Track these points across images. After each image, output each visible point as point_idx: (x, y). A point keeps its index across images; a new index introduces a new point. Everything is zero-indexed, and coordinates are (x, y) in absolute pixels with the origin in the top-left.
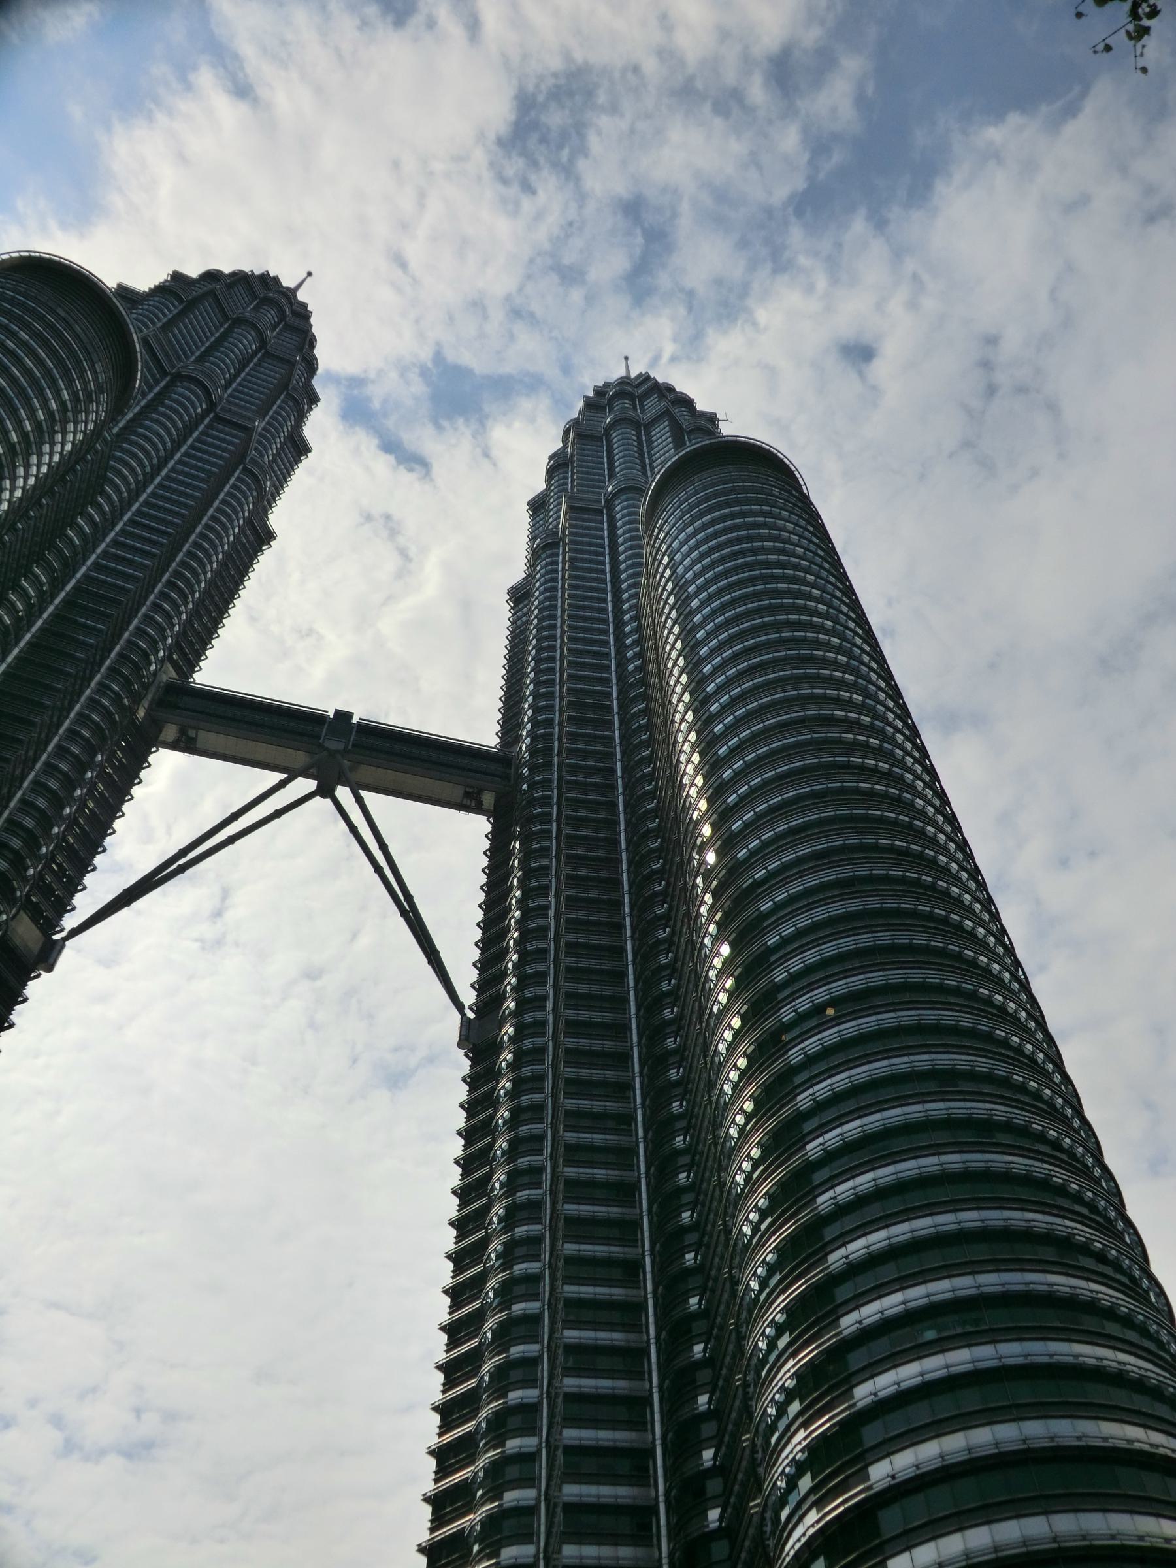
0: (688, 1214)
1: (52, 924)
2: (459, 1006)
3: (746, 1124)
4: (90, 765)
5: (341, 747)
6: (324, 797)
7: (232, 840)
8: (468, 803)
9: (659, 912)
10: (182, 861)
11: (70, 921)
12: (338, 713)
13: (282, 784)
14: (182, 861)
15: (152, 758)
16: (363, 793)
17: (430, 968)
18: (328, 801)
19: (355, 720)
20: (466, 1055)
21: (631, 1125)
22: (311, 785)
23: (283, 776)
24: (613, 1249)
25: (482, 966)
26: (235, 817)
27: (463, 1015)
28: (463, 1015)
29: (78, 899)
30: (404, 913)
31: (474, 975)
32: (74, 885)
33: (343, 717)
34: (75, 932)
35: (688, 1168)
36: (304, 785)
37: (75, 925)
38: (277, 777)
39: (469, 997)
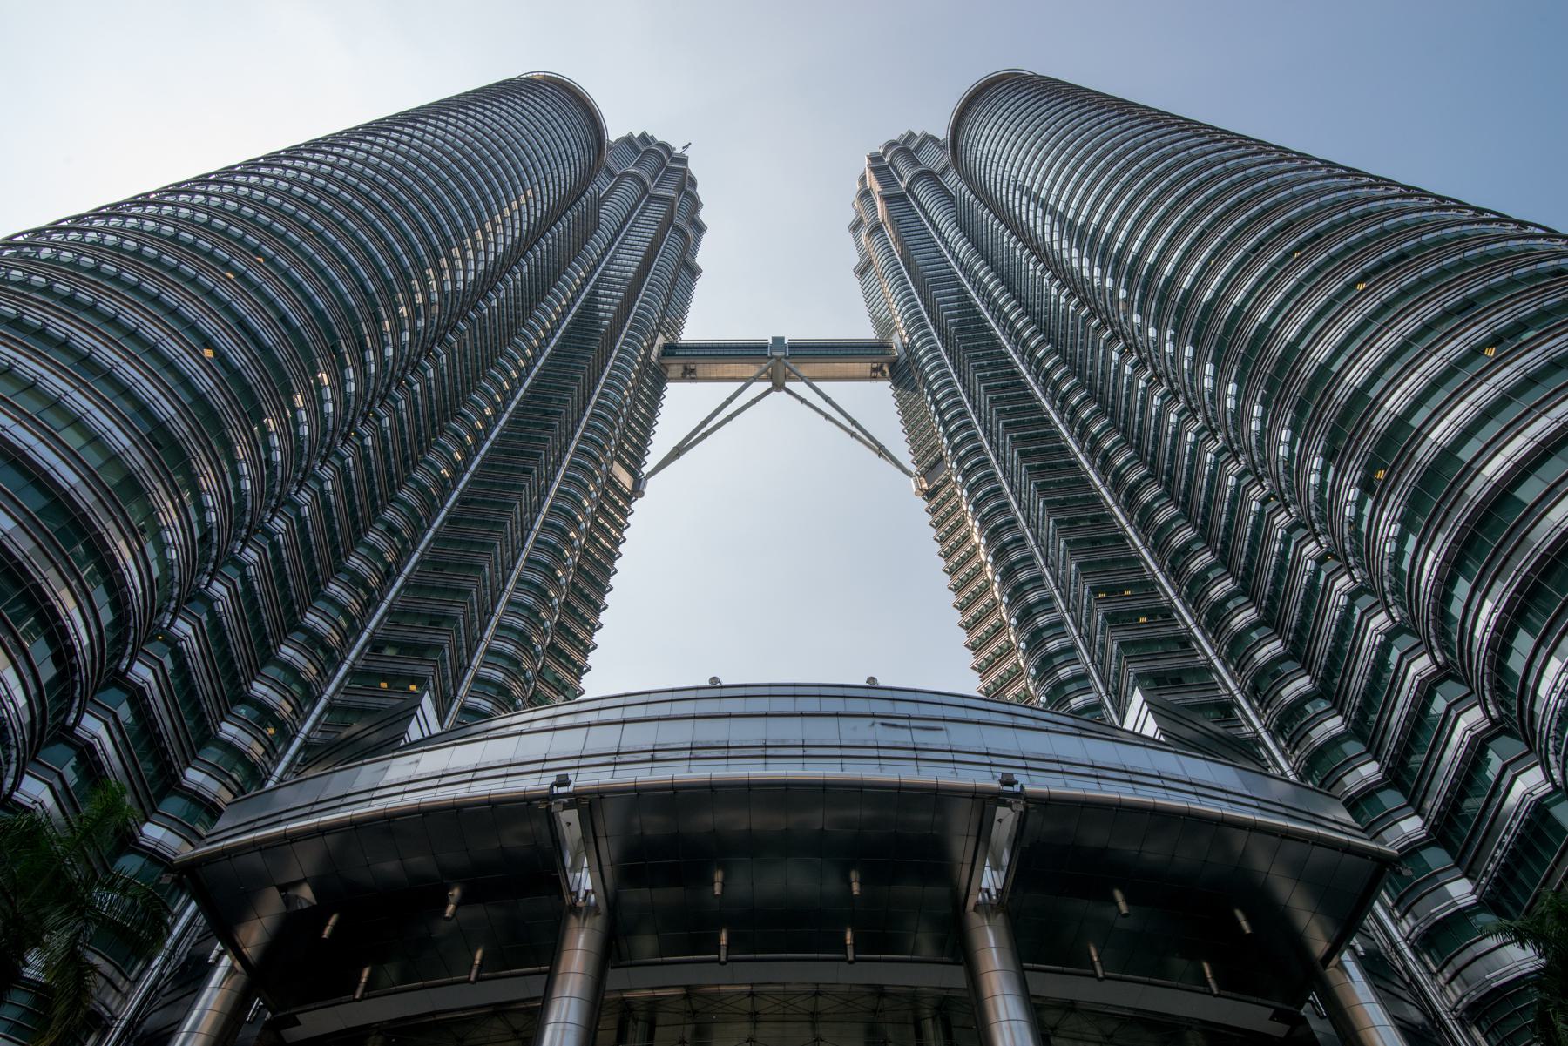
5: (783, 354)
7: (730, 417)
10: (704, 430)
11: (646, 470)
12: (774, 339)
14: (704, 430)
17: (882, 459)
18: (783, 393)
19: (786, 342)
22: (769, 385)
30: (853, 435)
33: (778, 341)
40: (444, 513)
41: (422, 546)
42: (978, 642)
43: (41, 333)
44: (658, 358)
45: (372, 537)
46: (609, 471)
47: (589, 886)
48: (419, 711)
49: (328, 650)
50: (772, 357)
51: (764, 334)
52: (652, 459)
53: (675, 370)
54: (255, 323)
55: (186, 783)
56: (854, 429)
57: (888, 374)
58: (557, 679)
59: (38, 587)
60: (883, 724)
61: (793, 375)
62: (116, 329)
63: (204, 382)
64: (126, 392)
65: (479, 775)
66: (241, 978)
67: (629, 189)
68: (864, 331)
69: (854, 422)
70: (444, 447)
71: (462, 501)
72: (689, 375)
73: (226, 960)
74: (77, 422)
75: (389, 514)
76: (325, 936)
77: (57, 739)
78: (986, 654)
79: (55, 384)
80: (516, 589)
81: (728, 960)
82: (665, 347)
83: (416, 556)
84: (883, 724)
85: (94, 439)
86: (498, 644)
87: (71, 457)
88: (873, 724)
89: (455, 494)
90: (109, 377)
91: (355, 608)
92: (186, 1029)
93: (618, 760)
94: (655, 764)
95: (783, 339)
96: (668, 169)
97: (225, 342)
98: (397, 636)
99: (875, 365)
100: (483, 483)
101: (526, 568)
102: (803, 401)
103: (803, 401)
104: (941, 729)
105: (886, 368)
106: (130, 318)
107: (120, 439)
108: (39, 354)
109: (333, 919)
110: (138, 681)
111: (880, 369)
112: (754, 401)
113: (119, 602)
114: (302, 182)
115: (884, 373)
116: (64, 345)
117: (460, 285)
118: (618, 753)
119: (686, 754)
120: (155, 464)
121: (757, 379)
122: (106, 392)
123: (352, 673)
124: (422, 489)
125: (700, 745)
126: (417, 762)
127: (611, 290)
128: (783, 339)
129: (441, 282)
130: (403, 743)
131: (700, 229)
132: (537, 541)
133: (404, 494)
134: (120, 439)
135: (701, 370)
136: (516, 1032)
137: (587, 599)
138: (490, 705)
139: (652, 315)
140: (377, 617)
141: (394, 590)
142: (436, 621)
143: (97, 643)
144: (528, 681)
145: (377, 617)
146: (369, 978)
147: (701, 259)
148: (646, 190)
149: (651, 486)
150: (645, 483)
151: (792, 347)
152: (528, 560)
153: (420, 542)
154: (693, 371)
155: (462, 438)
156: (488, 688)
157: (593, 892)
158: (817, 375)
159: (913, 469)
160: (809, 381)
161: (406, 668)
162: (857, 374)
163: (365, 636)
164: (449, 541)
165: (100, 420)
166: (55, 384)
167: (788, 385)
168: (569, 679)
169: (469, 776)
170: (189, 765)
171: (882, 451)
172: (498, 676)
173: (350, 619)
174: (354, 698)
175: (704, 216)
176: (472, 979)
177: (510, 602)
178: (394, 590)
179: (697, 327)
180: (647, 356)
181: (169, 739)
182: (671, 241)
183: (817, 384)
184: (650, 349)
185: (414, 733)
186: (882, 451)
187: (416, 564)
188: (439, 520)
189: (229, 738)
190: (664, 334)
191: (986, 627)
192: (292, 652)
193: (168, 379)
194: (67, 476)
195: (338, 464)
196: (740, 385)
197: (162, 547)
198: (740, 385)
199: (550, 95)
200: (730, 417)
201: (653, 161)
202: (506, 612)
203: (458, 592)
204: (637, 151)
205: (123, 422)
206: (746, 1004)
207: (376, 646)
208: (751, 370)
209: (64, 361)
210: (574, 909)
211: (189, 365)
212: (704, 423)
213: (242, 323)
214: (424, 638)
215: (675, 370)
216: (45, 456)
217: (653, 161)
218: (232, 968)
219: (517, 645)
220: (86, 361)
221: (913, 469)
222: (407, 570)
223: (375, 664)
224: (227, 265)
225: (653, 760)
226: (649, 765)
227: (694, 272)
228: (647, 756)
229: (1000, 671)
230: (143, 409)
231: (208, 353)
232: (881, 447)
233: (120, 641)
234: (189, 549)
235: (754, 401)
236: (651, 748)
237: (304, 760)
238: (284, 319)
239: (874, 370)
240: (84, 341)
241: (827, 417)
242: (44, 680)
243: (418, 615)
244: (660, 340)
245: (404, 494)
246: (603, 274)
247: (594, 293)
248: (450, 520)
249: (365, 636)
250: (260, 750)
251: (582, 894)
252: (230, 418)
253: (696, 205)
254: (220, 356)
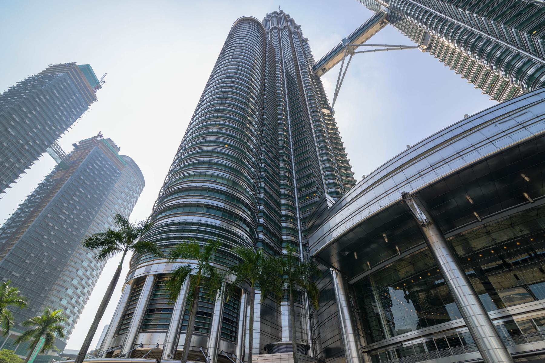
5: (348, 43)
7: (345, 73)
10: (339, 83)
11: (331, 105)
12: (343, 41)
14: (339, 83)
17: (403, 50)
18: (356, 54)
19: (347, 38)
22: (350, 55)
30: (387, 50)
33: (344, 40)
34: (333, 105)
40: (292, 149)
41: (293, 161)
42: (480, 84)
43: (199, 163)
44: (313, 73)
45: (281, 165)
46: (322, 112)
47: (425, 218)
48: (327, 199)
49: (290, 196)
51: (339, 41)
52: (330, 102)
53: (320, 72)
54: (230, 133)
55: (284, 239)
56: (387, 48)
57: (387, 22)
58: (345, 174)
59: (236, 213)
60: (499, 123)
61: (355, 47)
62: (209, 153)
63: (231, 153)
64: (220, 165)
65: (369, 204)
66: (340, 274)
67: (275, 32)
68: (371, 14)
69: (385, 46)
70: (281, 134)
71: (294, 144)
72: (324, 71)
73: (334, 272)
74: (217, 177)
75: (281, 158)
76: (356, 258)
77: (257, 242)
78: (487, 86)
79: (209, 171)
80: (321, 157)
81: (482, 220)
82: (313, 68)
83: (293, 164)
84: (499, 123)
85: (223, 178)
86: (326, 173)
87: (222, 184)
88: (495, 126)
89: (291, 143)
90: (215, 164)
91: (289, 184)
92: (336, 289)
93: (409, 181)
94: (422, 177)
95: (345, 38)
96: (280, 18)
97: (228, 141)
98: (302, 185)
99: (381, 22)
100: (295, 136)
101: (319, 151)
102: (364, 52)
103: (364, 52)
104: (527, 112)
105: (385, 20)
106: (210, 149)
107: (227, 175)
108: (202, 167)
109: (355, 254)
110: (262, 223)
111: (383, 22)
112: (348, 64)
113: (249, 209)
114: (213, 94)
115: (385, 23)
116: (204, 163)
117: (259, 91)
118: (407, 180)
119: (431, 169)
120: (235, 175)
121: (345, 57)
122: (217, 167)
123: (299, 199)
124: (283, 147)
125: (434, 164)
126: (349, 209)
127: (288, 65)
128: (345, 38)
129: (254, 94)
130: (329, 208)
131: (299, 27)
132: (317, 142)
133: (281, 151)
134: (227, 175)
135: (327, 66)
136: (410, 263)
137: (338, 149)
138: (334, 189)
140: (295, 183)
141: (294, 174)
142: (309, 176)
143: (251, 219)
144: (339, 178)
145: (295, 183)
146: (370, 264)
147: (305, 36)
148: (279, 29)
149: (335, 108)
150: (333, 109)
152: (319, 148)
153: (292, 160)
154: (325, 69)
155: (283, 129)
156: (331, 185)
157: (427, 219)
158: (363, 40)
159: (417, 45)
160: (362, 44)
161: (310, 191)
162: (376, 30)
163: (295, 189)
164: (298, 156)
165: (221, 174)
166: (209, 171)
167: (355, 51)
168: (348, 172)
169: (367, 206)
170: (281, 235)
171: (401, 47)
172: (331, 181)
173: (290, 187)
174: (303, 204)
175: (297, 23)
176: (400, 254)
177: (321, 161)
178: (294, 174)
180: (310, 74)
181: (275, 232)
183: (365, 43)
184: (310, 72)
185: (330, 205)
186: (401, 47)
187: (294, 166)
188: (292, 152)
189: (285, 226)
190: (310, 65)
191: (481, 77)
192: (284, 201)
193: (224, 156)
194: (224, 189)
195: (264, 153)
196: (342, 61)
197: (248, 193)
198: (342, 61)
199: (242, 25)
200: (345, 73)
201: (275, 19)
202: (322, 164)
203: (309, 166)
204: (269, 21)
205: (224, 171)
206: (484, 230)
207: (299, 190)
208: (341, 55)
209: (207, 166)
210: (423, 225)
211: (226, 151)
212: (338, 81)
213: (228, 135)
214: (309, 181)
215: (320, 72)
216: (218, 187)
217: (275, 19)
218: (336, 273)
219: (331, 171)
220: (209, 163)
221: (417, 45)
222: (293, 168)
223: (302, 194)
224: (216, 124)
225: (421, 176)
226: (421, 178)
227: (305, 41)
228: (418, 175)
229: (497, 88)
230: (225, 166)
231: (226, 146)
232: (400, 46)
233: (254, 216)
234: (252, 190)
235: (348, 64)
236: (417, 173)
237: (303, 223)
238: (234, 128)
239: (381, 24)
240: (207, 159)
241: (375, 51)
242: (249, 231)
243: (304, 177)
244: (311, 67)
245: (281, 151)
246: (285, 62)
247: (286, 69)
248: (295, 150)
249: (295, 189)
250: (293, 225)
251: (424, 221)
252: (240, 157)
253: (292, 21)
254: (229, 145)
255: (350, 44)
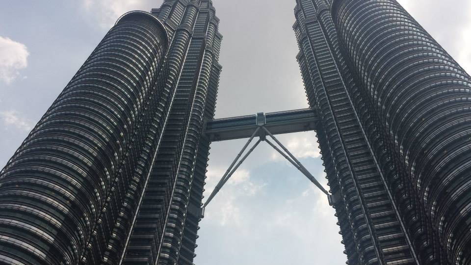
0: (426, 243)
1: (199, 204)
2: (326, 192)
3: (436, 209)
4: (194, 154)
5: (263, 124)
6: (263, 140)
8: (306, 128)
9: (381, 144)
11: (204, 201)
13: (250, 141)
15: (210, 146)
16: (274, 136)
19: (264, 114)
20: (333, 207)
21: (395, 217)
22: (258, 138)
23: (249, 138)
24: (404, 260)
25: (328, 177)
26: (240, 155)
27: (328, 195)
28: (328, 195)
29: (204, 194)
30: (299, 168)
31: (327, 181)
32: (202, 190)
33: (261, 115)
35: (421, 227)
36: (257, 139)
37: (205, 202)
38: (245, 140)
39: (328, 188)
50: (258, 126)
95: (262, 114)
102: (275, 147)
112: (252, 150)
139: (208, 68)
151: (268, 116)
179: (221, 112)
182: (205, 57)
235: (252, 150)
255: (263, 127)
